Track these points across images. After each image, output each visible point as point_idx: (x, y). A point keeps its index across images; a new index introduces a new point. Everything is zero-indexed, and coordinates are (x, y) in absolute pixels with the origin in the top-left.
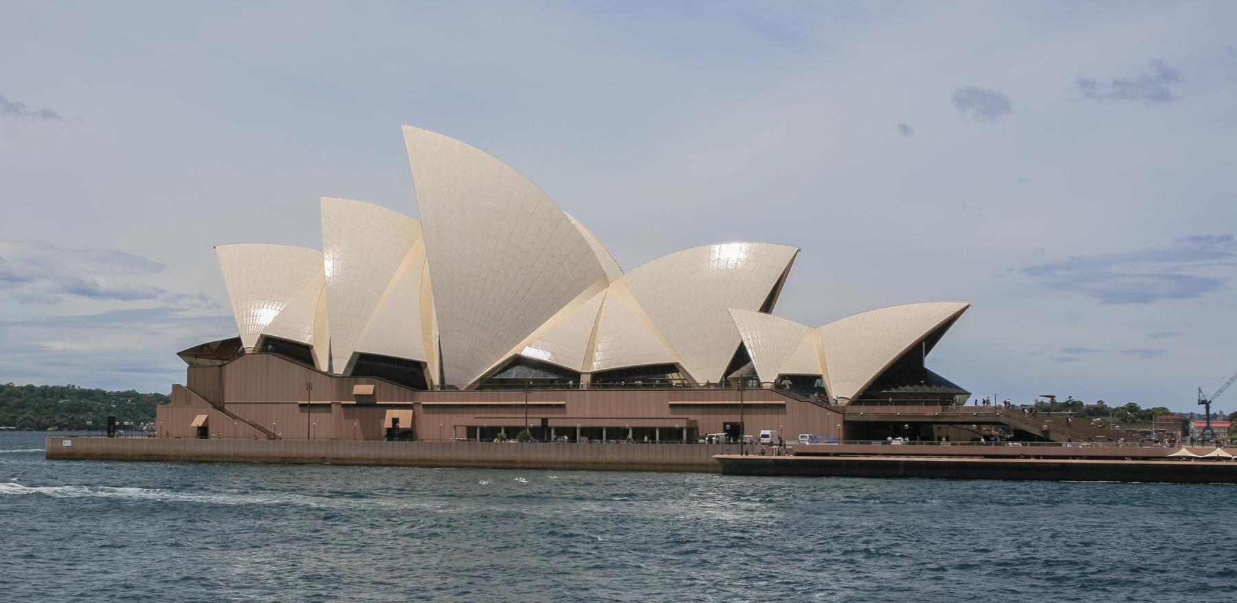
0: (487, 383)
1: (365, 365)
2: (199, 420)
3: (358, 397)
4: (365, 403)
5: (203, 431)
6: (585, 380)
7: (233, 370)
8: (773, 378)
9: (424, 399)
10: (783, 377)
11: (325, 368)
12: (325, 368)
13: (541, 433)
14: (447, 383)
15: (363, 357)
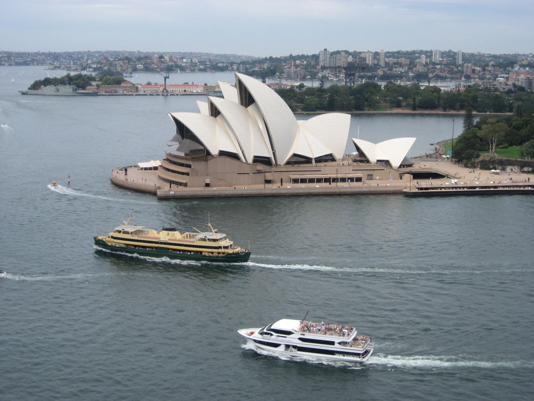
0: (288, 163)
1: (258, 160)
2: (208, 181)
3: (257, 170)
4: (259, 172)
5: (207, 185)
6: (314, 161)
7: (211, 162)
8: (375, 161)
9: (274, 169)
10: (378, 161)
11: (244, 161)
12: (244, 161)
13: (319, 180)
14: (278, 163)
15: (255, 157)
